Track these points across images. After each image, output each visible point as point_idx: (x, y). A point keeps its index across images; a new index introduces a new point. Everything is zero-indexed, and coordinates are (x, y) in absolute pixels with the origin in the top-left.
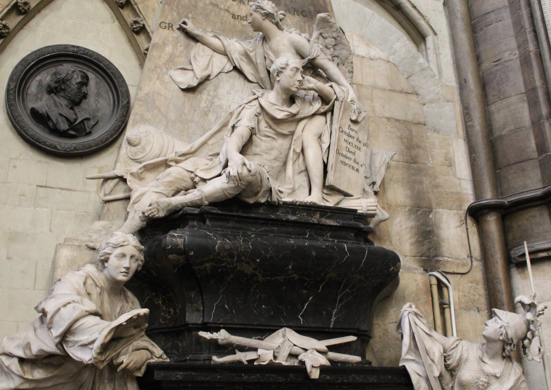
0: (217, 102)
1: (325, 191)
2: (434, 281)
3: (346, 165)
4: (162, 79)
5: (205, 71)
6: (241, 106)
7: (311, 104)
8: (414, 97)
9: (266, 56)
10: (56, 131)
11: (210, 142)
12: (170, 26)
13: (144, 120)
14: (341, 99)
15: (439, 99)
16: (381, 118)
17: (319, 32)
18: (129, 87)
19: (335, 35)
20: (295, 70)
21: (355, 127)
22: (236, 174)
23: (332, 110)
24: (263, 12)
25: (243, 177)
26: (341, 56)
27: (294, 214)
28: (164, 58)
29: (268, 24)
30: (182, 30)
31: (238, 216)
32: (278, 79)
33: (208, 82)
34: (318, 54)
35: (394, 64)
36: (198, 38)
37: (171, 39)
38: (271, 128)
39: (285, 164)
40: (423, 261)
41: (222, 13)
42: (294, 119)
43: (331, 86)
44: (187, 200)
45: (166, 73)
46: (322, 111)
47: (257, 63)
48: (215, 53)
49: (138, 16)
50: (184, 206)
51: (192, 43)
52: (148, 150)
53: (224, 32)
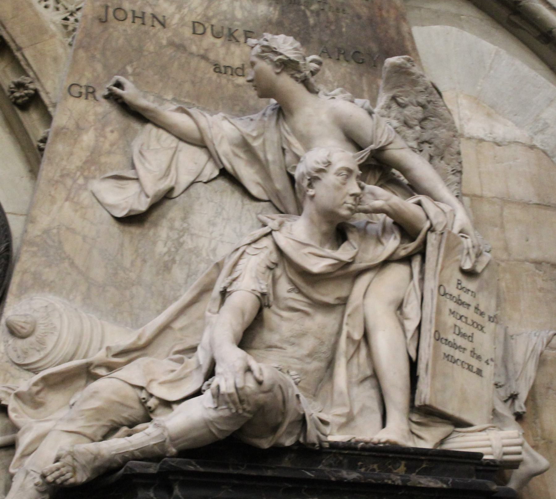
0: (189, 241)
1: (415, 418)
3: (455, 362)
4: (75, 200)
5: (162, 181)
6: (237, 249)
7: (379, 241)
9: (285, 147)
11: (177, 325)
14: (439, 229)
16: (523, 261)
17: (391, 94)
18: (10, 217)
19: (422, 99)
20: (345, 173)
21: (471, 285)
22: (232, 390)
23: (422, 252)
24: (276, 58)
25: (247, 396)
26: (436, 142)
27: (353, 467)
30: (113, 98)
31: (240, 477)
32: (311, 192)
33: (169, 203)
34: (390, 140)
35: (545, 152)
36: (147, 115)
37: (91, 118)
38: (300, 292)
39: (331, 364)
41: (194, 62)
43: (419, 204)
44: (132, 446)
45: (84, 187)
46: (403, 253)
47: (267, 160)
48: (182, 145)
49: (23, 72)
51: (136, 125)
52: (50, 346)
53: (198, 101)
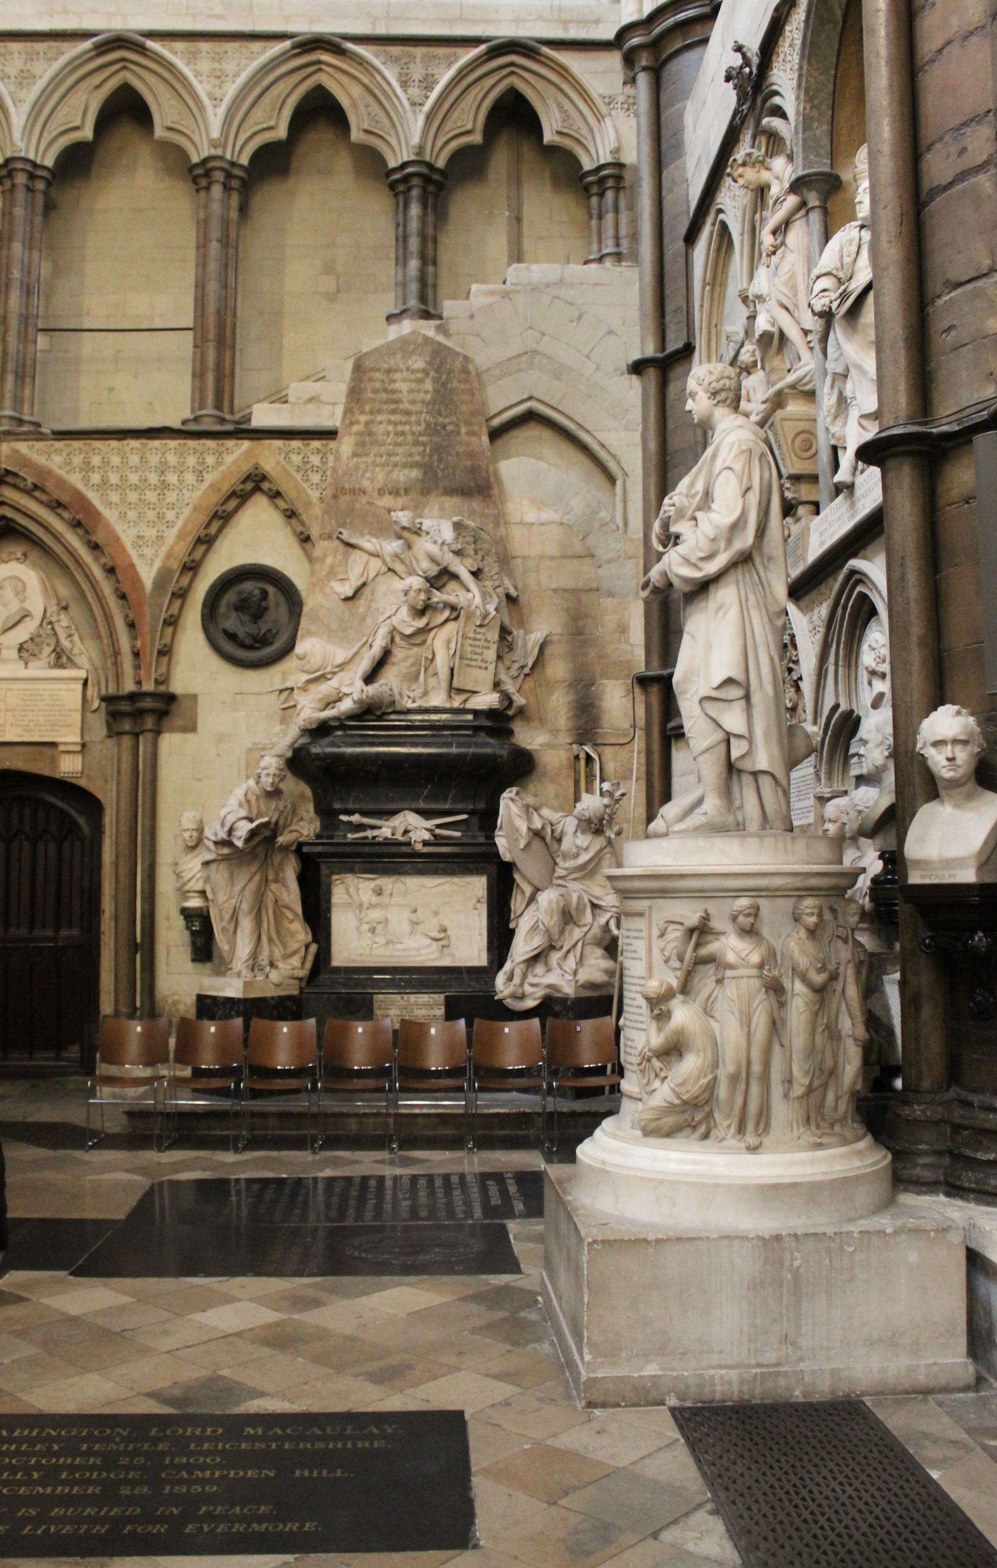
2: (582, 756)
8: (588, 561)
10: (243, 646)
12: (330, 537)
13: (310, 633)
21: (483, 630)
28: (326, 568)
29: (406, 534)
40: (579, 734)
42: (425, 630)
50: (330, 719)
51: (351, 550)
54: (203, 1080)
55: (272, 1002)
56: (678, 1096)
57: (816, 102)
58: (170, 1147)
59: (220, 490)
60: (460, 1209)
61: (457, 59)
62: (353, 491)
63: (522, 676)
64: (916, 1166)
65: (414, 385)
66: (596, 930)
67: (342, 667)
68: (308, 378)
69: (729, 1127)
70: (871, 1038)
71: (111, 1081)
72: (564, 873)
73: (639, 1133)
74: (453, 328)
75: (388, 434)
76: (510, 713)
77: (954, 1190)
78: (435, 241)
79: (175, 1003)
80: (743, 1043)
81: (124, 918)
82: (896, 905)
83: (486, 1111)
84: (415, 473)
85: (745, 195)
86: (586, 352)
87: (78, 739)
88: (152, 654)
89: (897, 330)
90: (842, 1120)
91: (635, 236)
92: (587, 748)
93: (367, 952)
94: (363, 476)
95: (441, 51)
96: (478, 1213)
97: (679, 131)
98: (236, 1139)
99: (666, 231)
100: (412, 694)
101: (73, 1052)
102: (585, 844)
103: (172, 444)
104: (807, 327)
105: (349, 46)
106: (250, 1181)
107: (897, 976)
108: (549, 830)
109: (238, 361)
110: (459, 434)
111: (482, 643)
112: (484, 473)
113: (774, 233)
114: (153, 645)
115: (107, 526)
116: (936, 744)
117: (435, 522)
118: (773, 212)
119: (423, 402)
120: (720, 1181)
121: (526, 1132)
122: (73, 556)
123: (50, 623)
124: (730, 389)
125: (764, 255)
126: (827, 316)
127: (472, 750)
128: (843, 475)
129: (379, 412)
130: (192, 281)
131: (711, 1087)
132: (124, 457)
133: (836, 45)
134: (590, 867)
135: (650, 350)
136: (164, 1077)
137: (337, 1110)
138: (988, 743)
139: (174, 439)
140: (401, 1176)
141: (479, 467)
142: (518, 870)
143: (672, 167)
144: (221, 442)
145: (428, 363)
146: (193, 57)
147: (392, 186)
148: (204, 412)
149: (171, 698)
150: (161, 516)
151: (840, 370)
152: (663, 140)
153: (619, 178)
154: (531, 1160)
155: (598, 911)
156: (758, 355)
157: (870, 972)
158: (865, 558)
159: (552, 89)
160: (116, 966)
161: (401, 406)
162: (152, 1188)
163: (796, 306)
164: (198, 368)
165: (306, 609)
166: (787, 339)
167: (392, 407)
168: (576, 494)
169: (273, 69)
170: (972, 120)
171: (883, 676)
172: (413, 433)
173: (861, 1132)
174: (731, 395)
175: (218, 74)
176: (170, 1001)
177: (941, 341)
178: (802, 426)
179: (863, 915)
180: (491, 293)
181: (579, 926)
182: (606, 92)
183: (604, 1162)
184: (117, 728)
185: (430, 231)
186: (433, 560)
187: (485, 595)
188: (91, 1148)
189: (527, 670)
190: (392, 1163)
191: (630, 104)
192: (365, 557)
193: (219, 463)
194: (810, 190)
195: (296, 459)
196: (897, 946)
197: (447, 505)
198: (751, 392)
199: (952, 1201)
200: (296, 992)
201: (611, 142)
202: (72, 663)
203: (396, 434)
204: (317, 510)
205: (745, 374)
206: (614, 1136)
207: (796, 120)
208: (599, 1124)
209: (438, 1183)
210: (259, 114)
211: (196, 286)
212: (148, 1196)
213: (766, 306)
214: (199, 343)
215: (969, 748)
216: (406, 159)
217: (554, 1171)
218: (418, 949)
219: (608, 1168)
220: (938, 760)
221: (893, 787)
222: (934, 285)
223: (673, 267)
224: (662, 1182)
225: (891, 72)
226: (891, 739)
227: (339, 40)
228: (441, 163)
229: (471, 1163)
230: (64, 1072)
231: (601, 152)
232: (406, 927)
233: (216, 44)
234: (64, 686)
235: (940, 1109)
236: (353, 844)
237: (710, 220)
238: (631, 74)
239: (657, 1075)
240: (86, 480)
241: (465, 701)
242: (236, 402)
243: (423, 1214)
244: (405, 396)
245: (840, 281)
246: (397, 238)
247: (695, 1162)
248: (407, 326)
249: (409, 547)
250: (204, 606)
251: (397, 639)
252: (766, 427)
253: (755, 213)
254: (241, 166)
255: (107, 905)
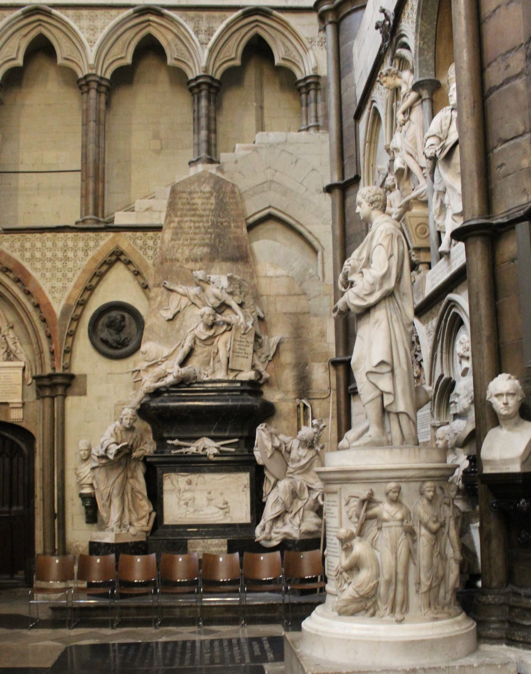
2: (301, 405)
8: (303, 297)
10: (111, 347)
12: (159, 286)
13: (149, 340)
15: (320, 295)
21: (245, 336)
28: (157, 303)
29: (201, 283)
35: (292, 277)
37: (160, 293)
42: (213, 337)
50: (161, 387)
51: (171, 293)
54: (93, 589)
55: (132, 545)
56: (358, 593)
57: (426, 40)
58: (76, 626)
59: (97, 260)
60: (237, 658)
61: (226, 18)
62: (172, 260)
63: (267, 362)
64: (490, 629)
65: (204, 201)
66: (311, 502)
67: (167, 358)
68: (145, 197)
69: (386, 609)
70: (464, 559)
71: (42, 590)
72: (292, 470)
73: (336, 614)
74: (226, 169)
75: (191, 228)
76: (261, 382)
77: (511, 642)
78: (215, 120)
79: (77, 546)
80: (393, 563)
81: (48, 499)
82: (477, 485)
83: (251, 603)
84: (206, 250)
85: (388, 92)
86: (300, 181)
87: (20, 400)
88: (61, 353)
89: (472, 166)
90: (449, 605)
91: (326, 116)
92: (304, 401)
93: (184, 516)
94: (177, 251)
95: (217, 14)
96: (248, 660)
97: (350, 57)
98: (113, 621)
99: (344, 112)
100: (206, 373)
101: (21, 575)
102: (304, 455)
103: (70, 235)
104: (423, 165)
105: (166, 11)
106: (121, 645)
107: (478, 524)
108: (283, 447)
109: (106, 189)
110: (230, 227)
111: (245, 344)
112: (244, 249)
113: (404, 113)
114: (61, 347)
115: (35, 281)
116: (497, 396)
117: (218, 276)
118: (403, 101)
119: (210, 210)
120: (382, 640)
121: (273, 615)
122: (15, 298)
123: (4, 336)
124: (380, 200)
125: (398, 125)
126: (434, 159)
127: (240, 403)
128: (443, 247)
129: (185, 215)
130: (80, 144)
131: (376, 587)
132: (43, 242)
133: (437, 9)
134: (307, 467)
135: (336, 179)
136: (71, 588)
137: (169, 604)
138: (526, 395)
139: (71, 232)
140: (205, 640)
141: (242, 246)
142: (267, 469)
143: (347, 77)
144: (97, 234)
145: (212, 188)
146: (78, 19)
147: (191, 90)
148: (88, 217)
149: (72, 377)
150: (64, 275)
151: (441, 189)
152: (341, 63)
153: (317, 84)
154: (277, 630)
155: (312, 491)
156: (396, 181)
157: (462, 524)
158: (457, 293)
159: (279, 35)
160: (44, 525)
161: (198, 213)
162: (66, 649)
163: (417, 154)
164: (84, 192)
165: (146, 326)
166: (412, 173)
167: (192, 213)
168: (296, 260)
169: (123, 24)
170: (512, 50)
171: (468, 358)
172: (205, 228)
173: (459, 611)
174: (381, 204)
175: (93, 28)
176: (74, 545)
177: (497, 172)
178: (420, 220)
179: (459, 491)
180: (247, 149)
181: (301, 500)
182: (310, 36)
183: (317, 631)
184: (41, 394)
185: (212, 115)
186: (217, 298)
187: (246, 317)
188: (32, 628)
189: (270, 358)
190: (200, 633)
191: (323, 43)
192: (179, 297)
193: (96, 246)
194: (423, 89)
195: (140, 242)
196: (478, 508)
197: (224, 267)
198: (392, 202)
199: (510, 648)
200: (144, 539)
201: (313, 64)
202: (16, 358)
203: (195, 228)
204: (152, 271)
205: (388, 192)
206: (322, 616)
207: (415, 51)
208: (314, 609)
209: (225, 643)
210: (116, 50)
211: (82, 146)
212: (64, 655)
213: (400, 154)
214: (84, 179)
215: (516, 397)
216: (198, 74)
217: (290, 636)
218: (212, 514)
219: (320, 634)
220: (499, 404)
221: (474, 419)
222: (493, 142)
223: (348, 133)
224: (349, 640)
225: (467, 24)
226: (473, 393)
227: (159, 8)
228: (218, 77)
229: (243, 632)
230: (16, 586)
231: (307, 69)
232: (205, 502)
233: (91, 11)
234: (12, 371)
235: (503, 597)
236: (176, 456)
237: (368, 106)
238: (323, 26)
239: (345, 582)
240: (22, 256)
241: (236, 376)
242: (106, 211)
243: (217, 660)
244: (200, 207)
245: (441, 140)
246: (194, 119)
247: (368, 629)
248: (200, 168)
249: (203, 290)
250: (90, 325)
251: (198, 342)
252: (401, 221)
253: (393, 102)
254: (106, 80)
255: (38, 492)
